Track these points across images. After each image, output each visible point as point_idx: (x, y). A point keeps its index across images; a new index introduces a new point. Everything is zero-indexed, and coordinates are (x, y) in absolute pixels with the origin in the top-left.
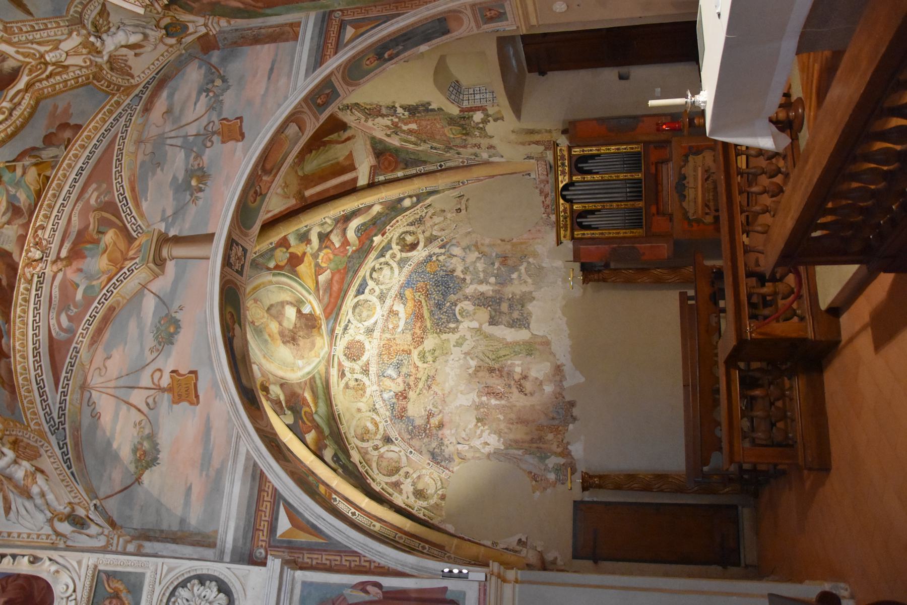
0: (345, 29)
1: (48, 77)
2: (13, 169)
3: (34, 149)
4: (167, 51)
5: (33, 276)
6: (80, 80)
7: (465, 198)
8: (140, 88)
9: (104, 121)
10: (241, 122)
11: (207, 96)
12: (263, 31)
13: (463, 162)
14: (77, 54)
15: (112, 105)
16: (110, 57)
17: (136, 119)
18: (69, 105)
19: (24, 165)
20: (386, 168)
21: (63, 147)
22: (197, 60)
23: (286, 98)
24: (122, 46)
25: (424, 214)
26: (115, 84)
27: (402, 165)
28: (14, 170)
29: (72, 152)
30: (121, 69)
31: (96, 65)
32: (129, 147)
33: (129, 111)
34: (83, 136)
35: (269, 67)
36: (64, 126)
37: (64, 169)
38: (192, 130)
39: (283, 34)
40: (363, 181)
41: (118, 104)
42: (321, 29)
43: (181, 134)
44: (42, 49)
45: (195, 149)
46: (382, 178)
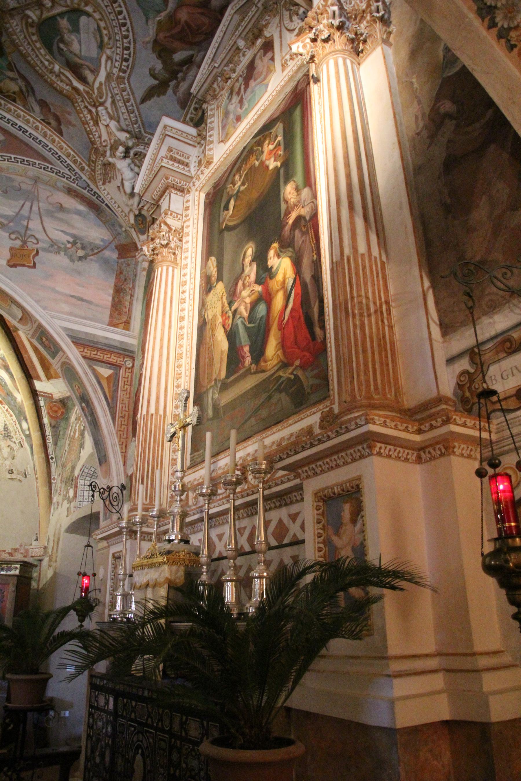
0: (110, 368)
3: (33, 91)
7: (22, 479)
8: (95, 189)
9: (68, 156)
10: (29, 267)
11: (69, 242)
12: (128, 298)
13: (54, 479)
14: (109, 134)
17: (62, 181)
18: (74, 126)
19: (17, 79)
20: (51, 408)
21: (42, 117)
22: (111, 238)
23: (45, 308)
25: (13, 440)
26: (95, 167)
27: (54, 423)
29: (40, 126)
32: (32, 171)
33: (73, 177)
34: (54, 137)
35: (85, 298)
37: (24, 116)
38: (35, 225)
39: (120, 314)
40: (39, 385)
41: (82, 169)
42: (115, 347)
43: (32, 215)
44: (108, 104)
45: (11, 224)
46: (42, 403)
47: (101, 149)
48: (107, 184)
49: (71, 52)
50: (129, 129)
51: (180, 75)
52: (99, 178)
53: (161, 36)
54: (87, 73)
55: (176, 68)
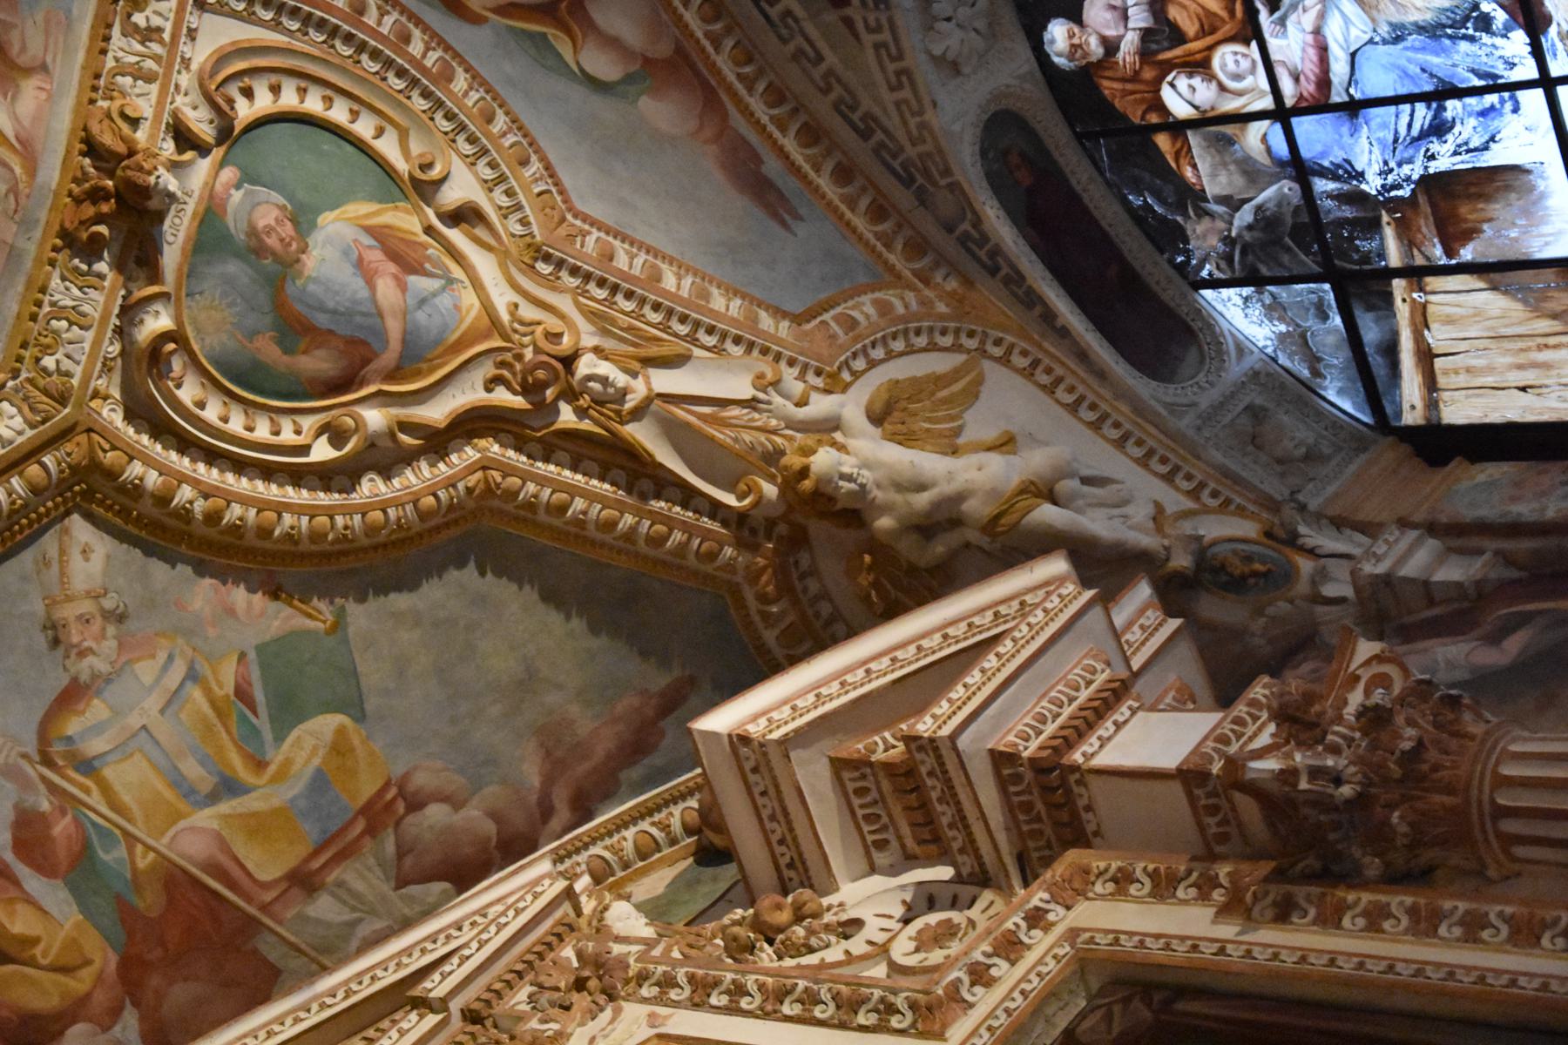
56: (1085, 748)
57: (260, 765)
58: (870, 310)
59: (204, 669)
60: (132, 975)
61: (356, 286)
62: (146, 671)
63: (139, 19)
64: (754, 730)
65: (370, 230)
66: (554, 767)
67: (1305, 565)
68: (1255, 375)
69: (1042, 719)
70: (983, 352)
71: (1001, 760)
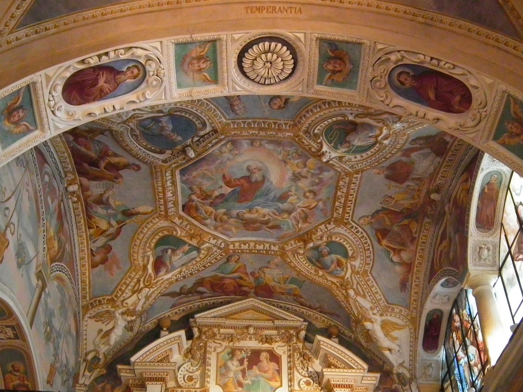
1: (139, 281)
2: (118, 223)
3: (113, 239)
4: (86, 349)
5: (66, 176)
6: (120, 293)
8: (81, 318)
14: (135, 304)
15: (86, 293)
16: (115, 317)
19: (113, 227)
24: (113, 328)
26: (97, 306)
28: (117, 222)
30: (101, 317)
31: (118, 306)
36: (104, 261)
37: (84, 239)
41: (84, 297)
44: (152, 290)
47: (117, 303)
48: (93, 320)
49: (170, 257)
50: (144, 306)
51: (191, 295)
52: (91, 312)
53: (210, 279)
54: (163, 271)
55: (193, 291)
56: (338, 389)
57: (285, 283)
58: (398, 310)
59: (284, 274)
60: (256, 288)
61: (329, 264)
62: (277, 270)
63: (327, 225)
64: (321, 343)
65: (337, 259)
66: (320, 307)
67: (408, 387)
68: (437, 361)
69: (338, 381)
70: (408, 326)
71: (329, 380)
